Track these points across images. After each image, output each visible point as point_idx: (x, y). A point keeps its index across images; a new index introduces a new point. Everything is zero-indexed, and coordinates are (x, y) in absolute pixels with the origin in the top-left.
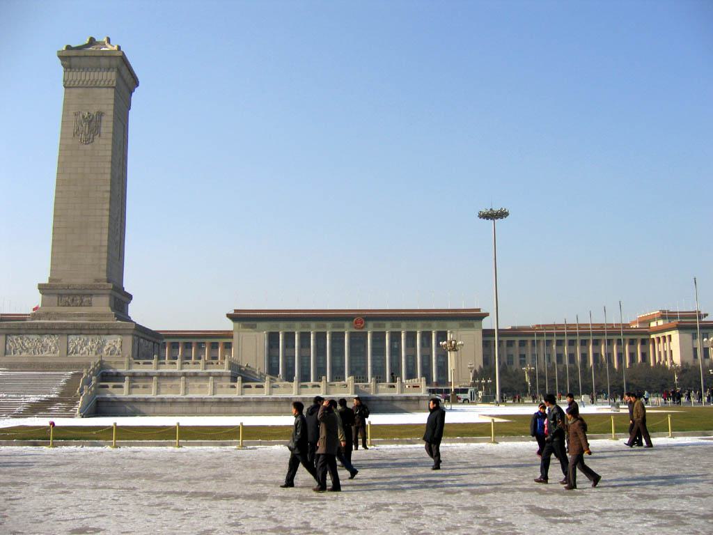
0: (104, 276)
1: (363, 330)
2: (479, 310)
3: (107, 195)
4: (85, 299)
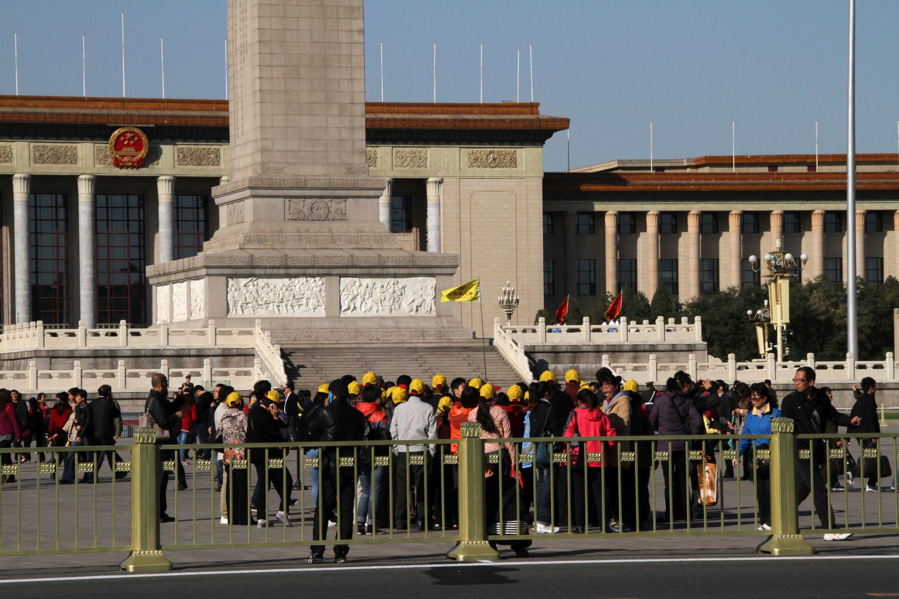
1: (144, 172)
2: (534, 106)
4: (334, 205)
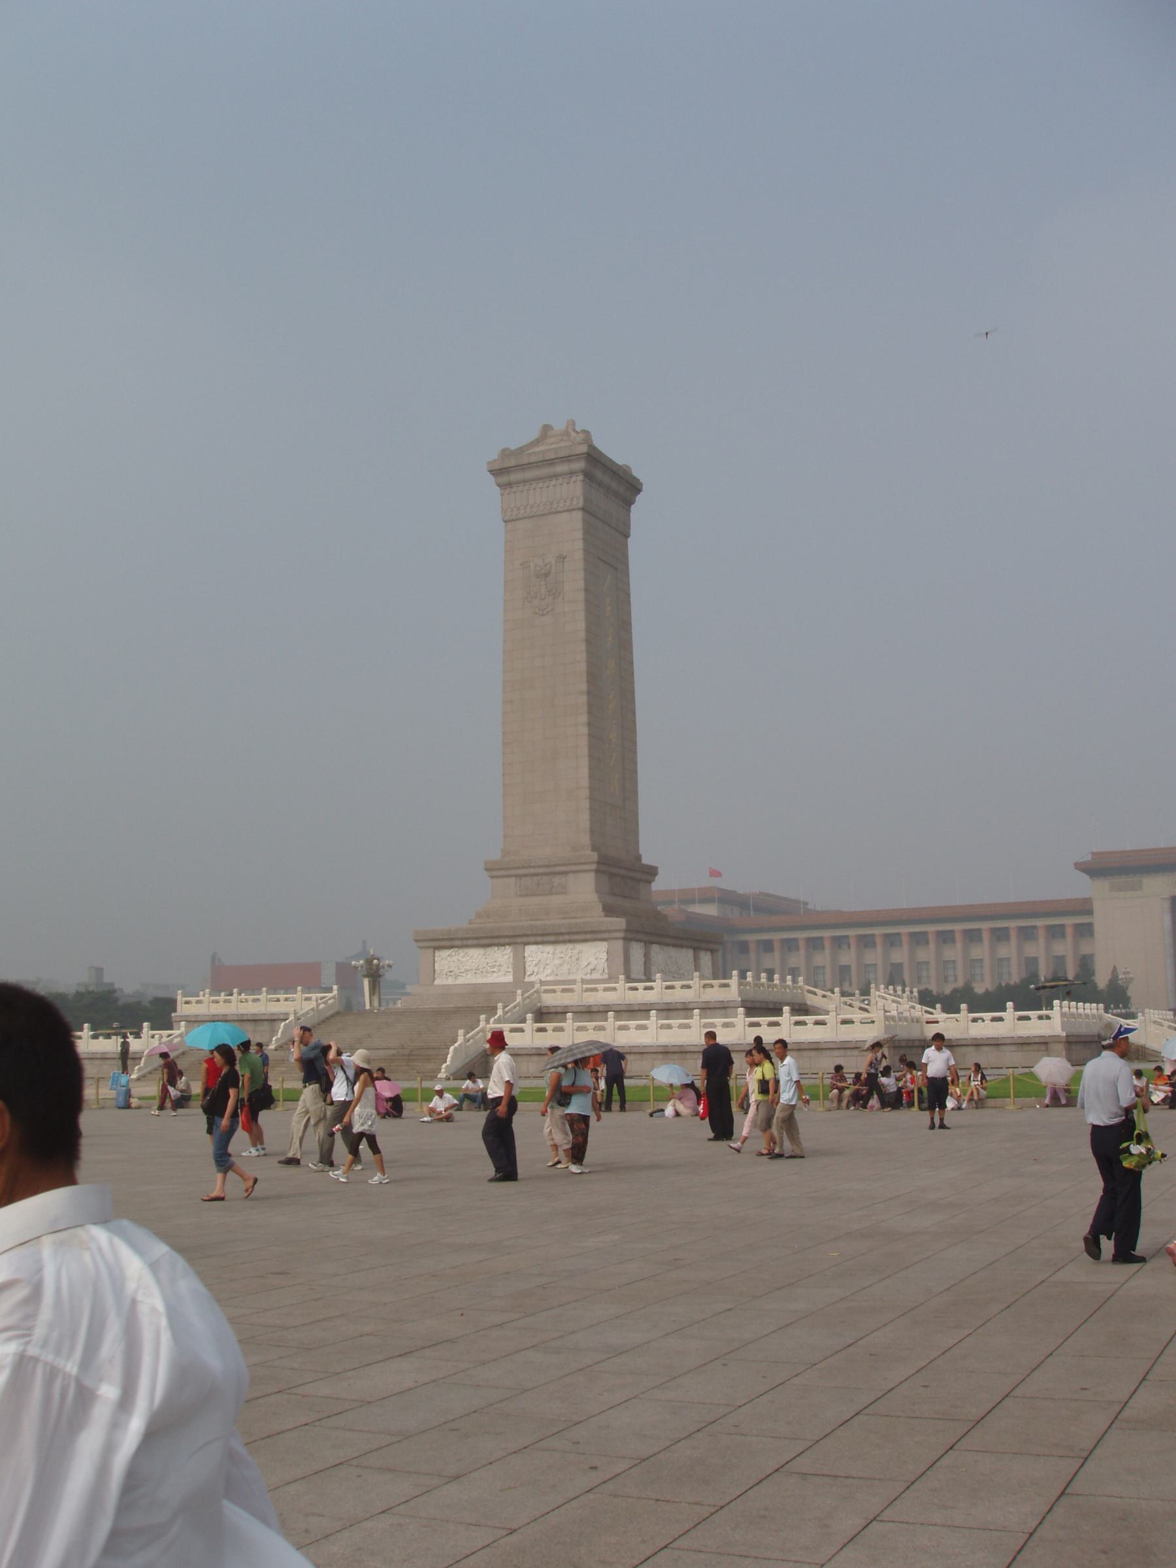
0: (585, 839)
3: (583, 699)
4: (557, 880)
